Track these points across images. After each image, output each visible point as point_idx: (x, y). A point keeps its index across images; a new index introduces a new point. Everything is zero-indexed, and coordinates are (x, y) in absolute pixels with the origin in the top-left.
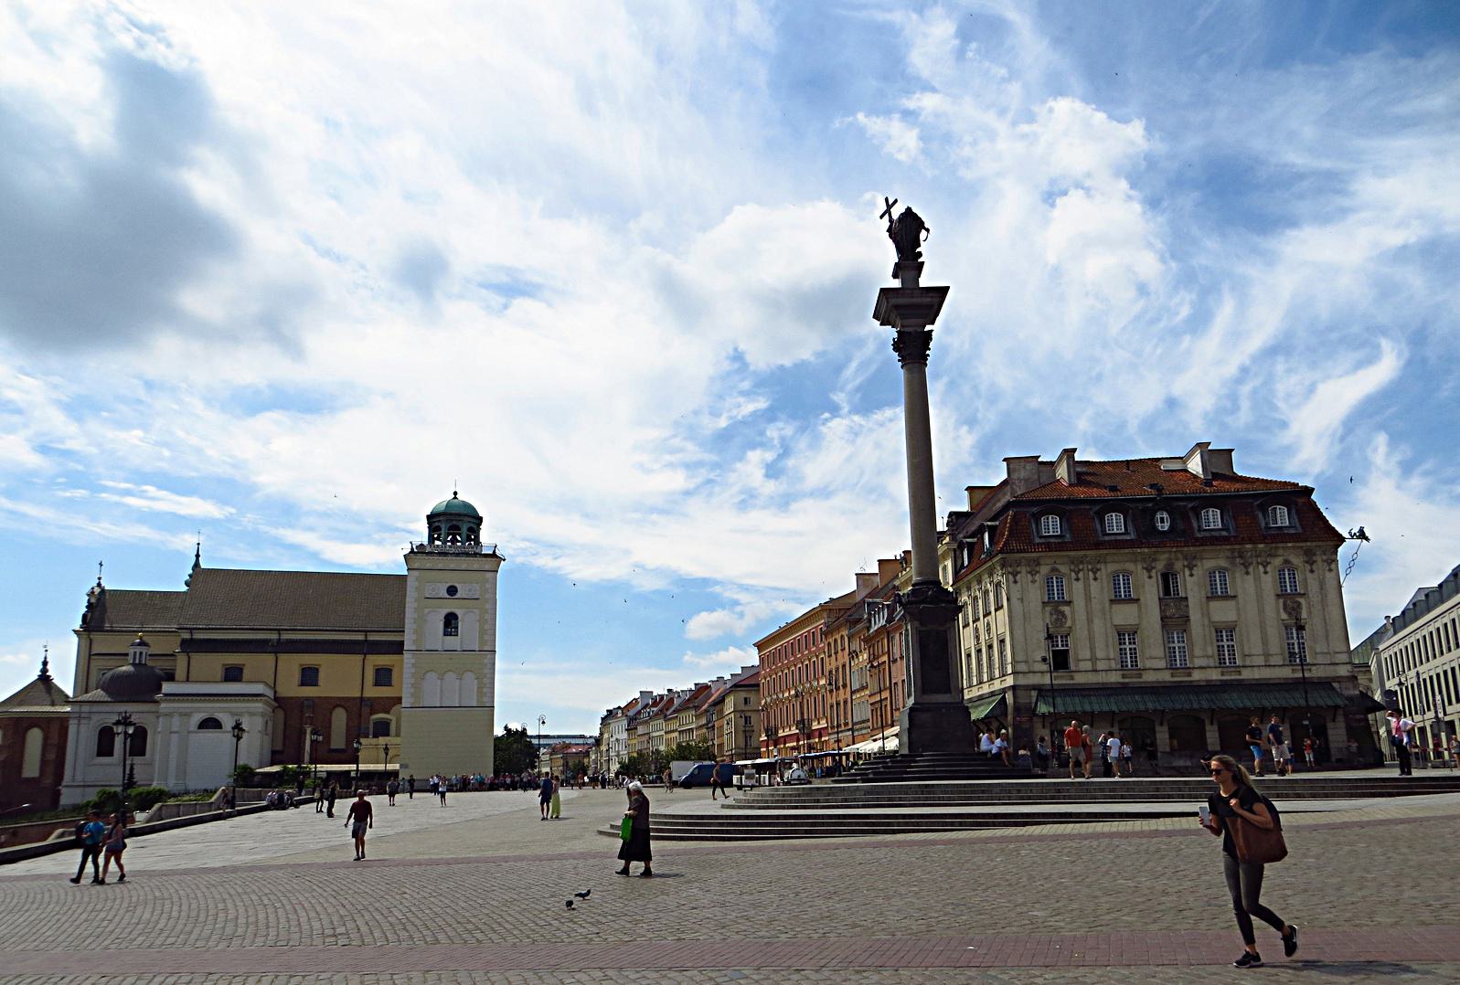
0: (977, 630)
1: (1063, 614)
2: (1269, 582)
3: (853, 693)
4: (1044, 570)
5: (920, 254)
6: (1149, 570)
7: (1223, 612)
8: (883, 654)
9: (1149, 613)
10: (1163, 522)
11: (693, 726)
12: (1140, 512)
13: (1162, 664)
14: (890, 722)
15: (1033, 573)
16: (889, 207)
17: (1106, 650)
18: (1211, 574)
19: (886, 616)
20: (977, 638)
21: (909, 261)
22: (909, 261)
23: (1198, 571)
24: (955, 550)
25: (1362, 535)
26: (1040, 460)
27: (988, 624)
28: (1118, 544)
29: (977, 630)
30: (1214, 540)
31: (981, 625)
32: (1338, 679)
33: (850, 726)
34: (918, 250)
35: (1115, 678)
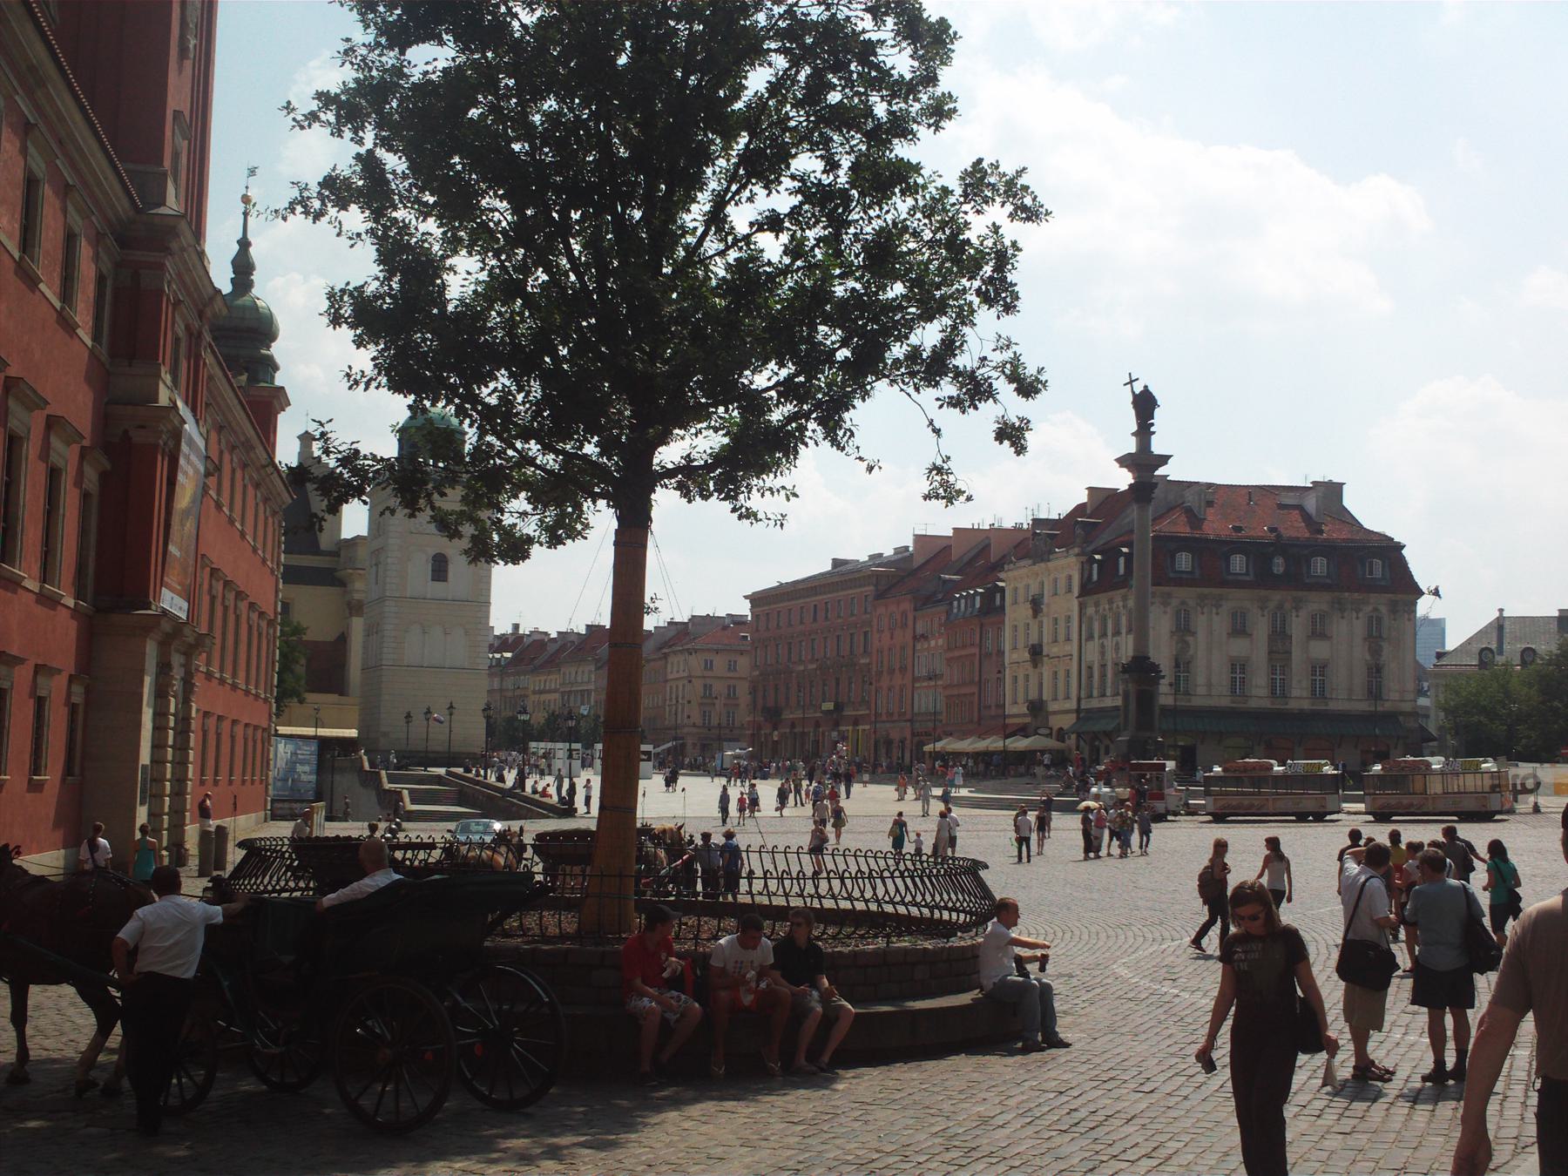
0: (1103, 646)
1: (1186, 643)
2: (1359, 626)
3: (915, 680)
4: (1175, 602)
6: (1262, 609)
7: (1320, 650)
9: (1256, 649)
10: (1279, 565)
11: (592, 687)
12: (1260, 552)
13: (1264, 692)
15: (1165, 604)
16: (1131, 382)
17: (1221, 678)
18: (1313, 617)
19: (978, 605)
20: (1103, 654)
21: (1144, 431)
22: (1144, 431)
23: (1303, 613)
25: (1436, 593)
28: (1239, 584)
29: (1103, 646)
30: (1320, 586)
32: (1402, 713)
33: (908, 717)
35: (1225, 702)
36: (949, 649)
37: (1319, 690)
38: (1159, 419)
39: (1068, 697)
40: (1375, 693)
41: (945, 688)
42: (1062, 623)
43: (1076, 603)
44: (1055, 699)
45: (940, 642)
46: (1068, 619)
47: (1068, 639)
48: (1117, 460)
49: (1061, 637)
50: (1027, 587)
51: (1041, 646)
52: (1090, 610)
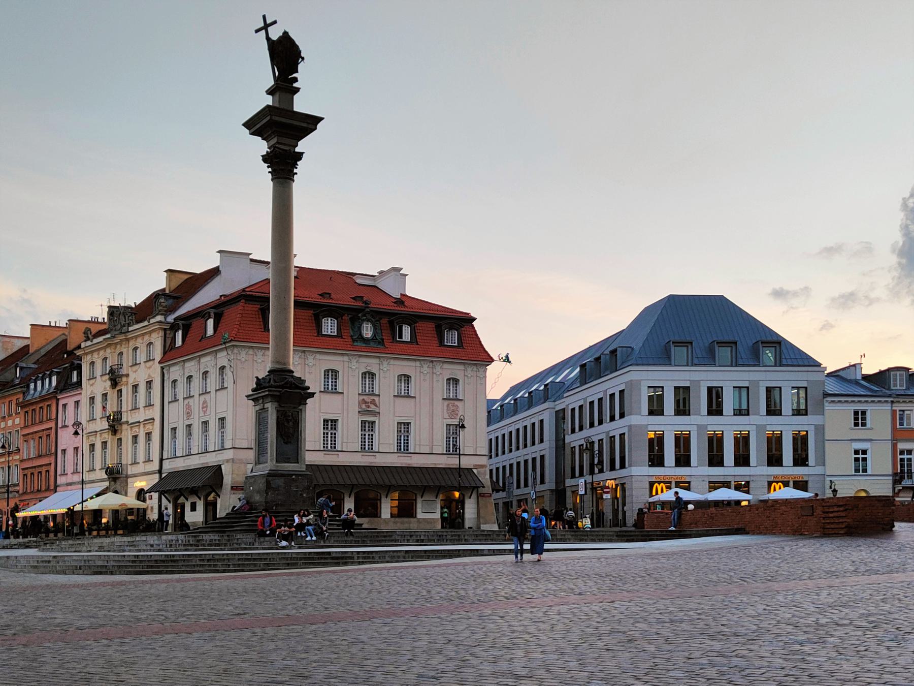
0: (189, 407)
5: (296, 80)
8: (49, 420)
14: (52, 487)
16: (266, 27)
19: (54, 383)
20: (189, 414)
21: (285, 85)
22: (285, 85)
24: (165, 330)
26: (251, 257)
27: (205, 402)
31: (195, 403)
34: (295, 75)
36: (25, 427)
37: (403, 446)
38: (304, 75)
39: (148, 460)
40: (454, 449)
41: (21, 461)
42: (142, 389)
43: (158, 367)
44: (135, 463)
45: (17, 421)
46: (149, 383)
47: (149, 405)
48: (248, 125)
49: (141, 402)
50: (105, 359)
51: (119, 413)
52: (175, 372)
